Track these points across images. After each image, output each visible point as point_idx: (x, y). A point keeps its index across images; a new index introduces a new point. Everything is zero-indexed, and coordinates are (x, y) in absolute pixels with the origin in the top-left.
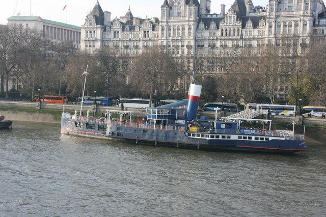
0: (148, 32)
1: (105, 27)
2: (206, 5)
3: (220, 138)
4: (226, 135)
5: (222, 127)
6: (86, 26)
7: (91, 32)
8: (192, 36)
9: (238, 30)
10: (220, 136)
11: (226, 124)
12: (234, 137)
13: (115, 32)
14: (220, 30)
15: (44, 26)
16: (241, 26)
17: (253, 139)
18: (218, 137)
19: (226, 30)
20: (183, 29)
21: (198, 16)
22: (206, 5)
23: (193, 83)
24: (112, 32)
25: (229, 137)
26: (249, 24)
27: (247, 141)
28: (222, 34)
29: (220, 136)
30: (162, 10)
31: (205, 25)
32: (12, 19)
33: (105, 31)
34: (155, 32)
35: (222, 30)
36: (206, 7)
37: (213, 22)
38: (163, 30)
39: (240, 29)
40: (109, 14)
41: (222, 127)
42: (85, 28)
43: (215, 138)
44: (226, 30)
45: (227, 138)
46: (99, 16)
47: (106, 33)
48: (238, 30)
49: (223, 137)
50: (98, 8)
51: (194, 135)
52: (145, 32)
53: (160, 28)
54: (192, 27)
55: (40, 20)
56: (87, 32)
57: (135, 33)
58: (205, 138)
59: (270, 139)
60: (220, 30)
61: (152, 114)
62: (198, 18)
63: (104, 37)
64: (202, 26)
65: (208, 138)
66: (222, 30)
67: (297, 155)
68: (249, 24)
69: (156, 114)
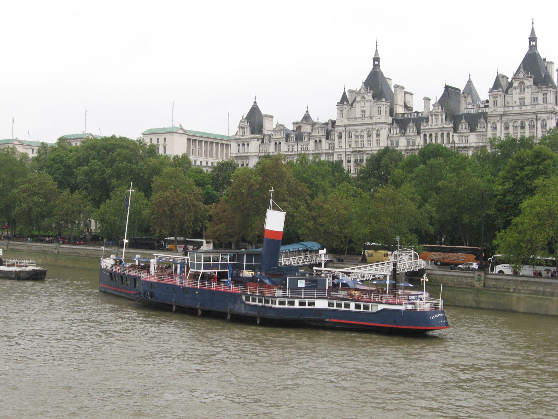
0: (320, 141)
1: (264, 137)
2: (405, 99)
3: (297, 305)
4: (307, 301)
6: (237, 137)
7: (244, 145)
9: (448, 134)
10: (297, 302)
11: (306, 280)
12: (321, 304)
14: (422, 135)
15: (189, 140)
16: (452, 129)
17: (352, 308)
18: (292, 303)
19: (431, 135)
20: (369, 136)
21: (391, 114)
22: (405, 99)
23: (274, 208)
24: (272, 144)
25: (312, 304)
26: (464, 126)
27: (352, 312)
28: (425, 140)
29: (297, 302)
31: (401, 128)
32: (151, 132)
33: (263, 142)
34: (330, 142)
35: (425, 135)
36: (405, 103)
37: (411, 124)
38: (340, 137)
39: (451, 133)
40: (270, 119)
42: (237, 139)
43: (287, 306)
44: (431, 135)
45: (333, 304)
47: (263, 145)
48: (448, 134)
49: (301, 304)
51: (254, 300)
53: (337, 134)
55: (181, 131)
56: (239, 145)
57: (302, 143)
58: (270, 305)
60: (422, 135)
61: (196, 262)
62: (391, 119)
64: (396, 130)
65: (274, 306)
66: (425, 135)
67: (434, 337)
68: (464, 126)
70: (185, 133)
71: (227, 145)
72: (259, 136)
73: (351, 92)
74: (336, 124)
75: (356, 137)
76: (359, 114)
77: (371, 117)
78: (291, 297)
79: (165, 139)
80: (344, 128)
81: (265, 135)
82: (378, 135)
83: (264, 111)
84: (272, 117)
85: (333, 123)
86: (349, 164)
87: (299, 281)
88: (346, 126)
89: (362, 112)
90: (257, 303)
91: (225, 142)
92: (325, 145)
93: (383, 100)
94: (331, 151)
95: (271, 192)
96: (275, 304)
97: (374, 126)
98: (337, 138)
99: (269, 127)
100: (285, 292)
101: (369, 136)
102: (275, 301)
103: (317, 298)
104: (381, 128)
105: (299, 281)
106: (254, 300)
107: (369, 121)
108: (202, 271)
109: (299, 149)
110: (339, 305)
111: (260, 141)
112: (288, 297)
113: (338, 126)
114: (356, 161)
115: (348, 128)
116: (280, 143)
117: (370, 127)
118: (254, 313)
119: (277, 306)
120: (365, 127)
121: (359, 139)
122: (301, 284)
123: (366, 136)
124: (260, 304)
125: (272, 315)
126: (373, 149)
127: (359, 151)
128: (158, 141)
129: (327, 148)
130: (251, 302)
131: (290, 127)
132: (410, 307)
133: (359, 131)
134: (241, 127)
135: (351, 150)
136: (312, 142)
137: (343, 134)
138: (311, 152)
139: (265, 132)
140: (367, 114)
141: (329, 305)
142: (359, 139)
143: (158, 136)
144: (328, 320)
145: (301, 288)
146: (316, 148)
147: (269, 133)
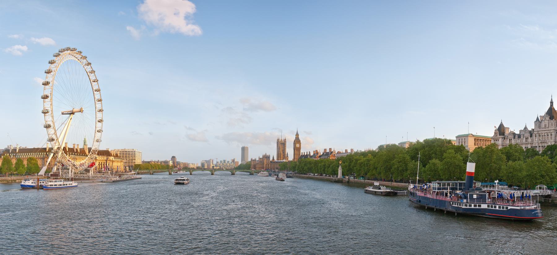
0: (528, 138)
3: (473, 207)
5: (474, 197)
8: (553, 139)
10: (473, 205)
12: (484, 206)
13: (510, 139)
15: (475, 139)
18: (470, 206)
20: (548, 135)
24: (508, 140)
29: (473, 205)
30: (535, 124)
32: (459, 136)
34: (532, 138)
41: (474, 197)
46: (501, 130)
49: (475, 206)
50: (501, 126)
52: (526, 138)
53: (534, 135)
54: (553, 134)
56: (495, 141)
58: (461, 206)
59: (509, 208)
63: (504, 143)
65: (462, 207)
69: (437, 187)
70: (473, 136)
71: (491, 140)
72: (503, 136)
73: (540, 116)
74: (534, 131)
75: (542, 136)
76: (543, 126)
77: (548, 127)
78: (470, 203)
79: (465, 139)
80: (537, 132)
81: (505, 136)
82: (551, 135)
83: (505, 126)
84: (509, 128)
85: (533, 130)
86: (540, 148)
87: (474, 195)
88: (538, 131)
89: (545, 125)
90: (456, 206)
91: (490, 140)
92: (530, 140)
93: (554, 120)
94: (532, 142)
95: (469, 154)
96: (463, 206)
97: (550, 131)
98: (534, 136)
99: (507, 133)
100: (467, 201)
101: (548, 135)
102: (463, 204)
103: (482, 204)
104: (553, 132)
105: (474, 195)
106: (455, 205)
107: (548, 129)
108: (437, 191)
109: (519, 142)
110: (492, 207)
111: (503, 139)
112: (469, 203)
113: (535, 132)
114: (542, 146)
115: (539, 132)
116: (511, 139)
117: (548, 131)
118: (454, 210)
119: (464, 207)
120: (546, 132)
121: (544, 137)
122: (475, 196)
123: (546, 135)
124: (457, 206)
125: (461, 211)
126: (550, 141)
127: (544, 142)
128: (462, 140)
129: (531, 141)
130: (454, 205)
131: (517, 132)
132: (522, 208)
133: (544, 133)
134: (495, 133)
135: (540, 141)
136: (525, 138)
137: (537, 135)
138: (524, 143)
139: (505, 135)
140: (547, 126)
141: (488, 207)
142: (544, 137)
143: (462, 138)
144: (487, 214)
145: (475, 199)
146: (526, 141)
147: (507, 135)
